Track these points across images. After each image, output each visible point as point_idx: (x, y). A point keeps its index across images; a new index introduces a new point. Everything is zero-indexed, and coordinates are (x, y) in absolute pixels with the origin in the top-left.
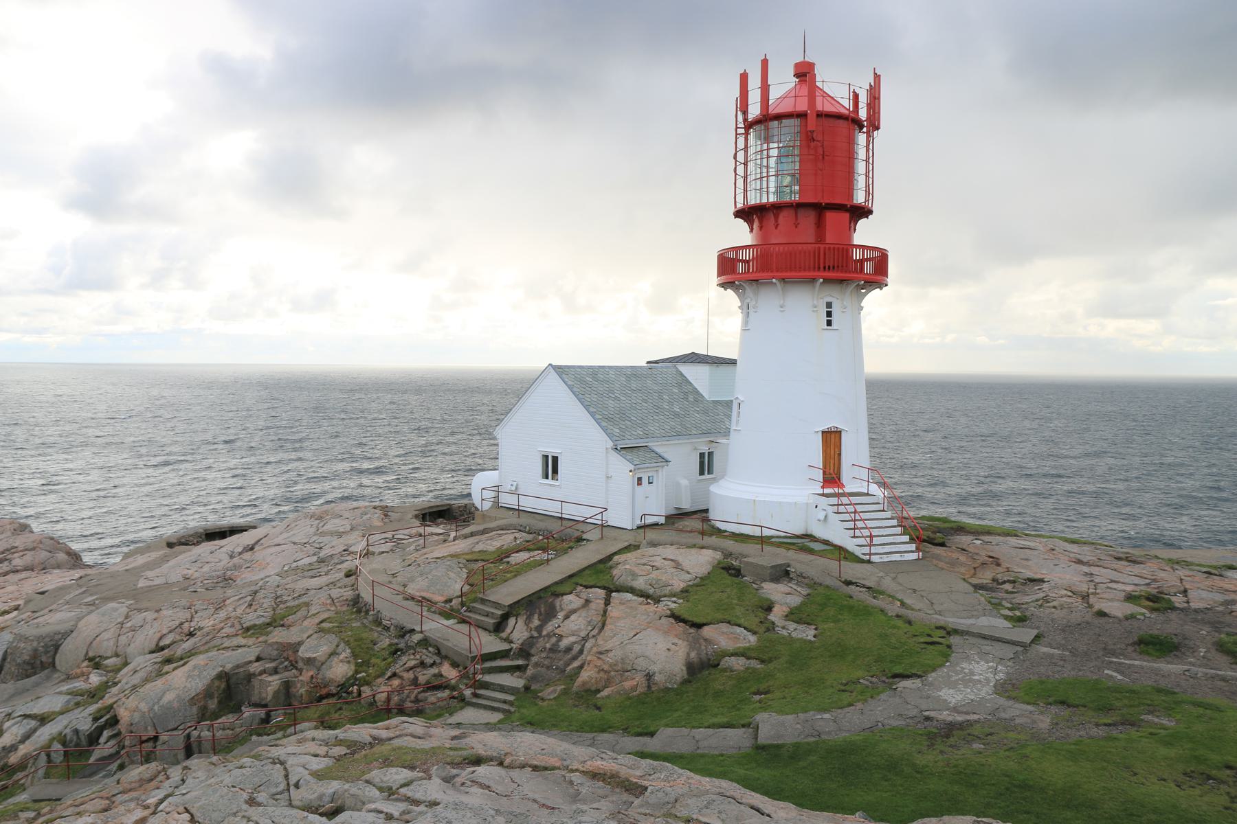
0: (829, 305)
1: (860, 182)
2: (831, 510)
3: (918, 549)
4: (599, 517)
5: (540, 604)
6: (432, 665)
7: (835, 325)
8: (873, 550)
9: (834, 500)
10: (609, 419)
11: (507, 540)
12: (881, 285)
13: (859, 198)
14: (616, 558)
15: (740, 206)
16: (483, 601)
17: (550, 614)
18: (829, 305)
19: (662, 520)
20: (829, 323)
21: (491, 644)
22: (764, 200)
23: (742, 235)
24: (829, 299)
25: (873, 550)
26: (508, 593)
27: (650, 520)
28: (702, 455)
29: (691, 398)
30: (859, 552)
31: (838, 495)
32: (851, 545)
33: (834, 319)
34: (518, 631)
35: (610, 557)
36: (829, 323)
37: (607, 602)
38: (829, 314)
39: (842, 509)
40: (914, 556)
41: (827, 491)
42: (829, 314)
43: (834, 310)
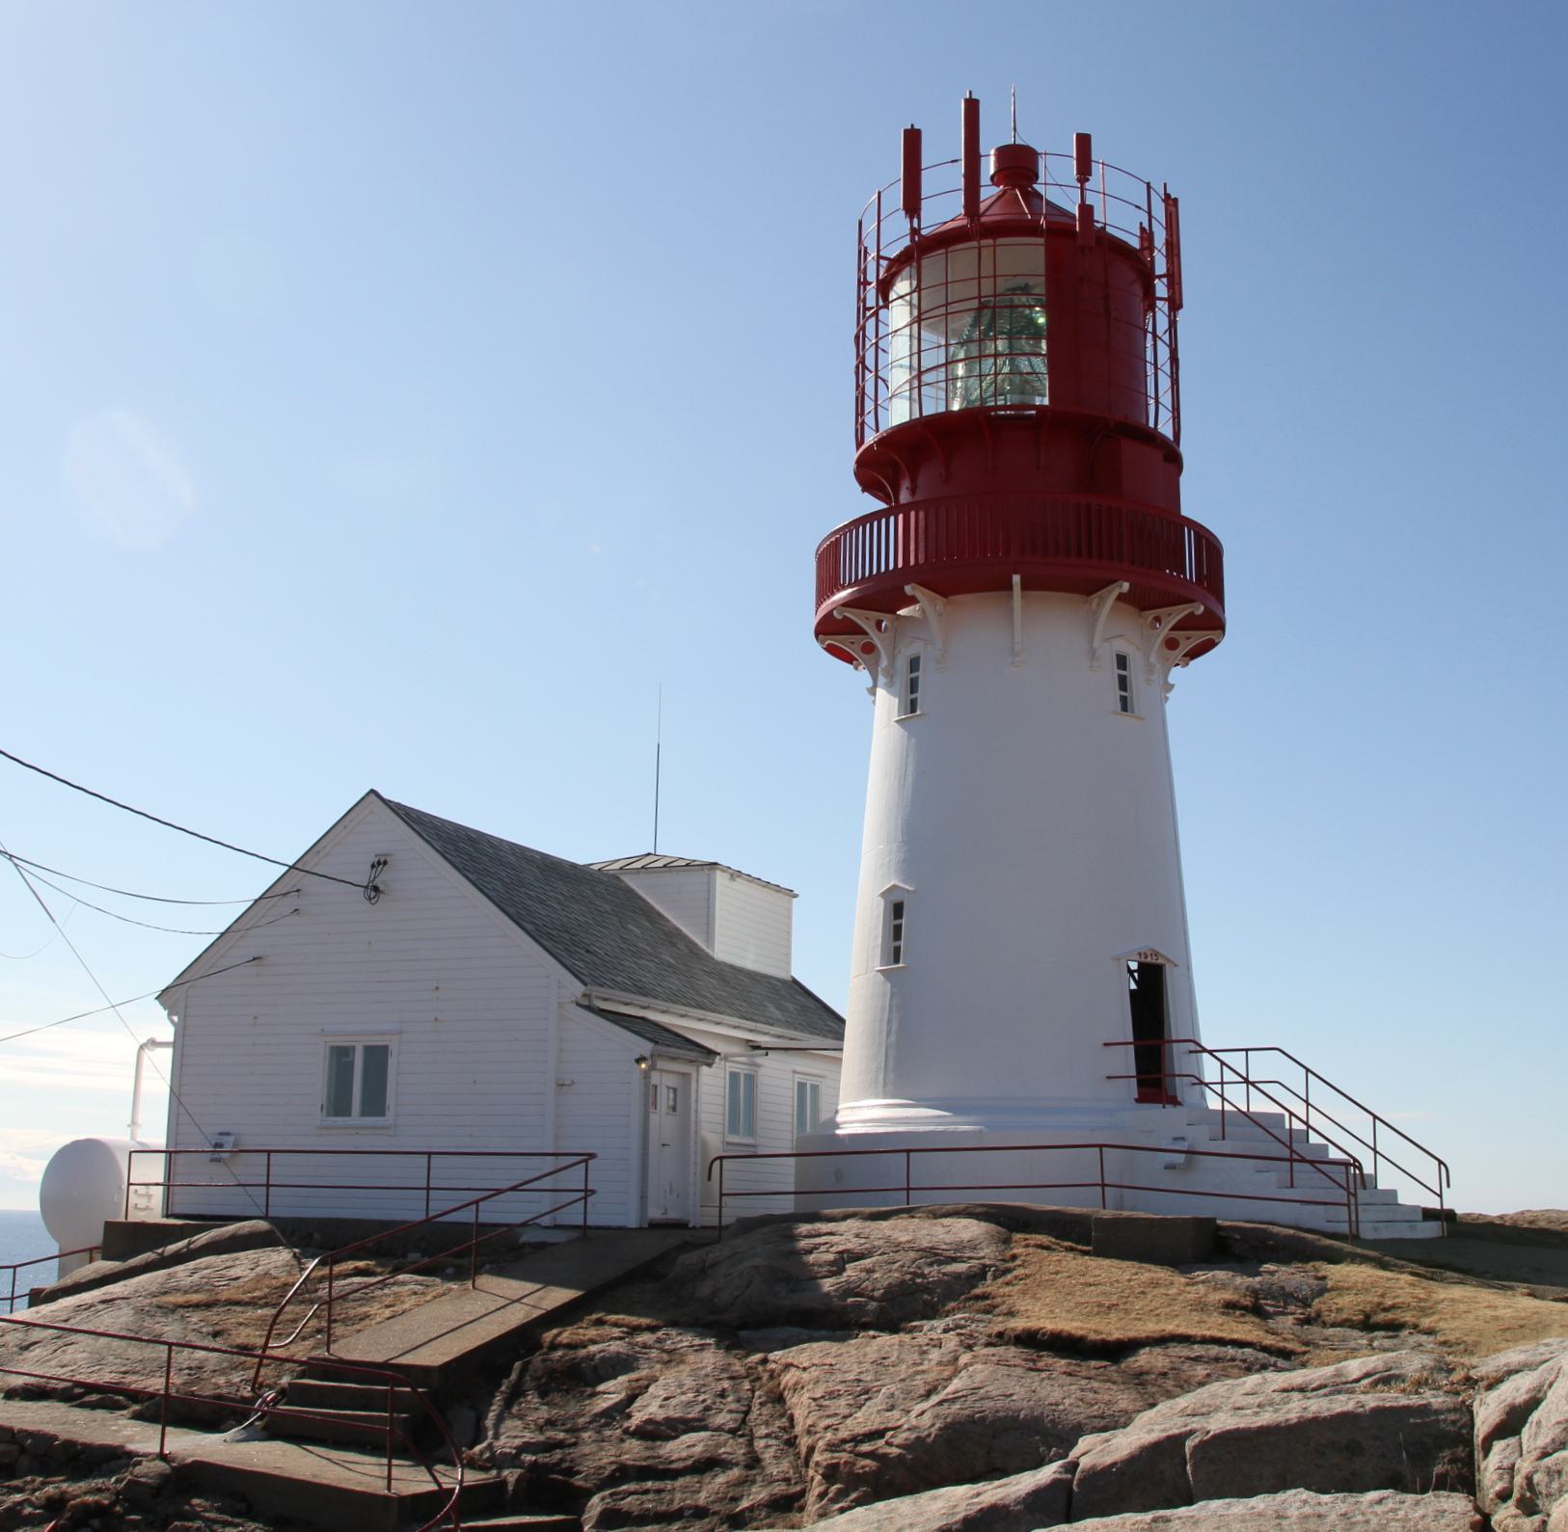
0: (1122, 661)
4: (574, 1178)
10: (551, 938)
13: (1166, 429)
18: (1122, 661)
20: (1125, 704)
24: (1121, 646)
36: (1125, 704)
38: (1123, 683)
42: (1123, 683)
43: (1135, 673)
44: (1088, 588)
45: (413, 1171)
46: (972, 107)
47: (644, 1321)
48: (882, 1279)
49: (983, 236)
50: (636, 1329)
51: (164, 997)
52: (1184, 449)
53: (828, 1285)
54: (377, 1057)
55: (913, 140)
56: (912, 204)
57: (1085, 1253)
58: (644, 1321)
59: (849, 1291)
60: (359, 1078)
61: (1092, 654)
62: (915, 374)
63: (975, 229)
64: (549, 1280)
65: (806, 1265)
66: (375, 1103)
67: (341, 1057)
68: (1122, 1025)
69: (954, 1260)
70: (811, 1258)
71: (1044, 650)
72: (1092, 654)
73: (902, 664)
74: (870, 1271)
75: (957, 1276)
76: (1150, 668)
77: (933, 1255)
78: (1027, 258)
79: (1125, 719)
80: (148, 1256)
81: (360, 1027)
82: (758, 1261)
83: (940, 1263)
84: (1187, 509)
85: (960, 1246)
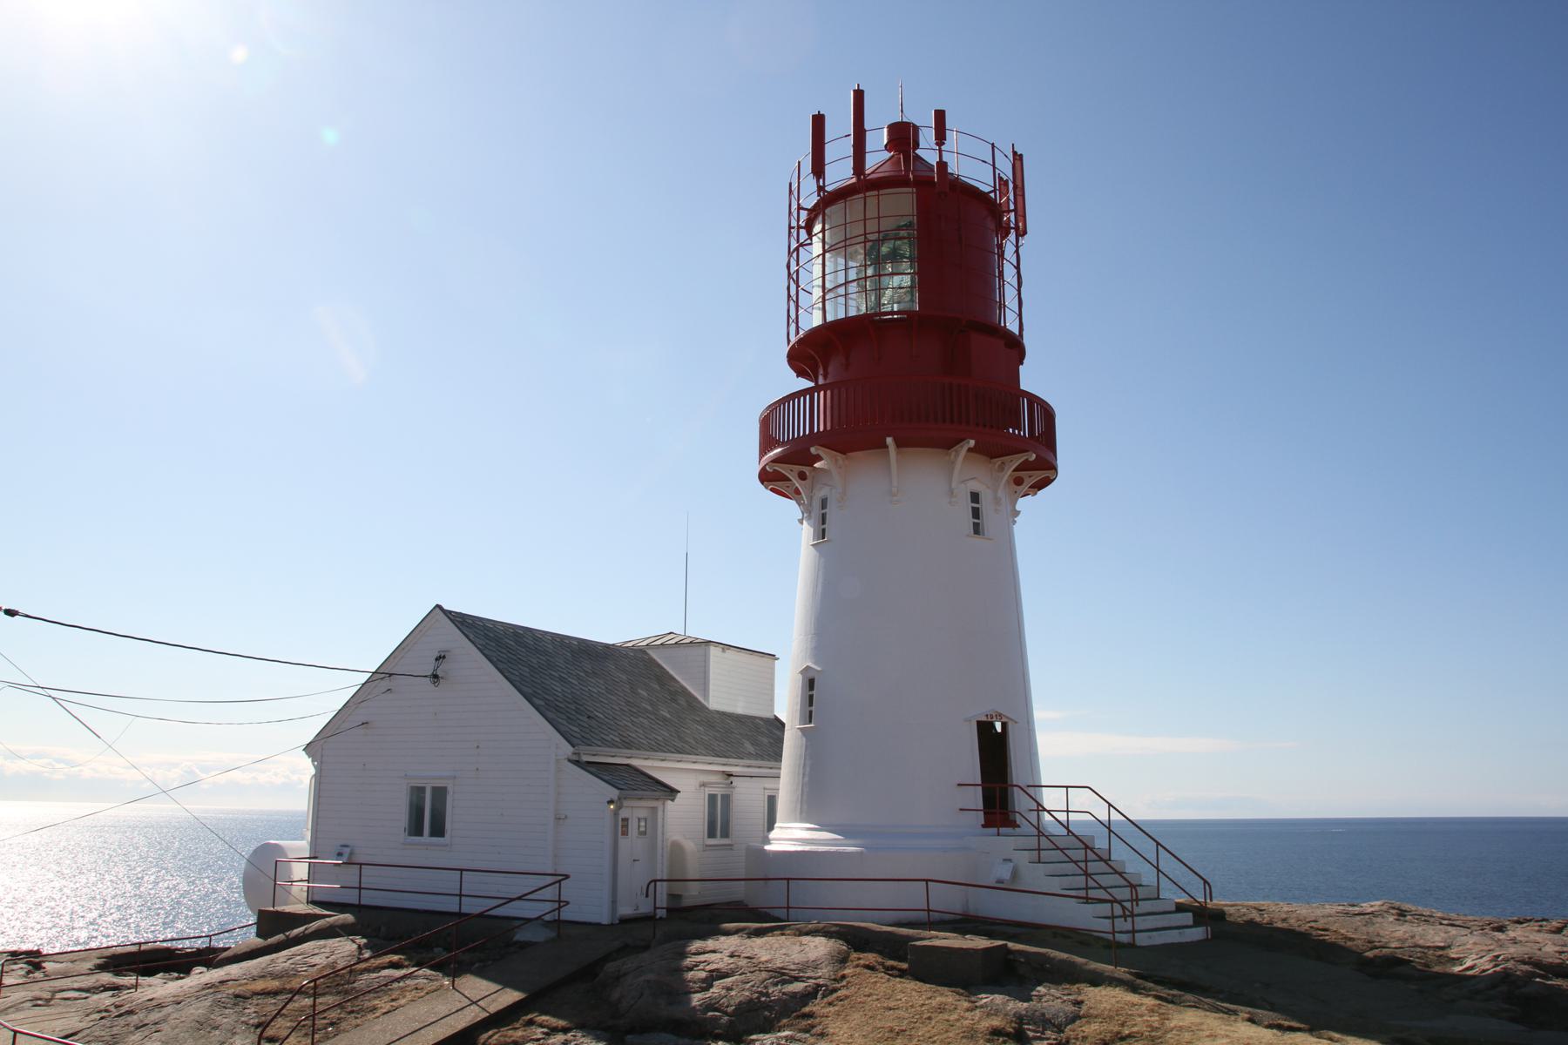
0: (975, 497)
3: (1196, 924)
4: (549, 893)
8: (1141, 923)
13: (1012, 326)
14: (610, 967)
18: (975, 497)
24: (975, 486)
25: (1141, 923)
28: (712, 798)
29: (682, 701)
35: (588, 972)
36: (977, 529)
38: (976, 513)
40: (1198, 934)
42: (976, 513)
43: (986, 505)
44: (948, 444)
45: (449, 882)
46: (859, 95)
47: (562, 1023)
48: (737, 996)
49: (868, 189)
50: (554, 1030)
51: (309, 749)
52: (1027, 341)
53: (696, 999)
54: (440, 794)
55: (819, 122)
56: (818, 169)
57: (902, 974)
58: (562, 1023)
59: (710, 1006)
60: (427, 815)
61: (951, 492)
62: (830, 289)
63: (864, 185)
64: (507, 983)
65: (684, 981)
66: (438, 830)
67: (418, 792)
69: (797, 979)
70: (690, 975)
71: (918, 491)
72: (951, 492)
73: (817, 504)
74: (729, 989)
75: (794, 995)
76: (997, 501)
77: (782, 975)
78: (902, 204)
79: (977, 540)
80: (281, 937)
81: (430, 774)
82: (651, 976)
83: (784, 982)
84: (1025, 385)
85: (804, 966)
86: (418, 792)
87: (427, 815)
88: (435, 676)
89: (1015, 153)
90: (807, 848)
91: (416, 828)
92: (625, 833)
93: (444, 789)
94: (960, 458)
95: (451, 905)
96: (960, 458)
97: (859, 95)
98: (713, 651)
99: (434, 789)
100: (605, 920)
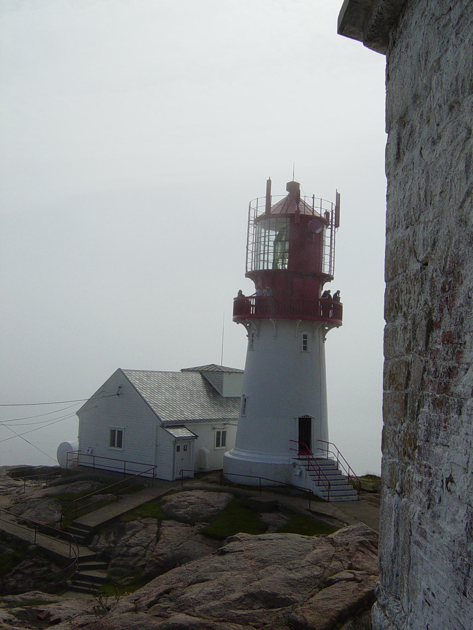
0: (305, 337)
1: (326, 259)
2: (303, 468)
5: (115, 525)
6: (43, 565)
7: (309, 349)
9: (306, 462)
11: (87, 486)
12: (338, 325)
14: (164, 498)
15: (249, 270)
16: (75, 525)
17: (122, 531)
18: (305, 337)
19: (192, 474)
20: (305, 348)
21: (84, 552)
22: (265, 268)
23: (250, 289)
24: (305, 333)
26: (92, 520)
27: (186, 474)
28: (218, 433)
30: (320, 494)
31: (309, 459)
32: (317, 491)
33: (309, 346)
34: (102, 543)
36: (305, 348)
37: (159, 525)
38: (305, 342)
39: (311, 468)
41: (301, 457)
42: (305, 342)
43: (309, 340)
45: (122, 465)
46: (269, 182)
54: (120, 433)
60: (117, 438)
66: (120, 445)
67: (113, 432)
68: (296, 435)
82: (172, 503)
86: (113, 432)
87: (117, 438)
88: (118, 394)
89: (337, 193)
90: (238, 458)
91: (113, 444)
92: (178, 450)
93: (122, 432)
94: (298, 325)
95: (123, 471)
96: (298, 325)
97: (269, 182)
98: (226, 377)
99: (118, 431)
100: (171, 479)
